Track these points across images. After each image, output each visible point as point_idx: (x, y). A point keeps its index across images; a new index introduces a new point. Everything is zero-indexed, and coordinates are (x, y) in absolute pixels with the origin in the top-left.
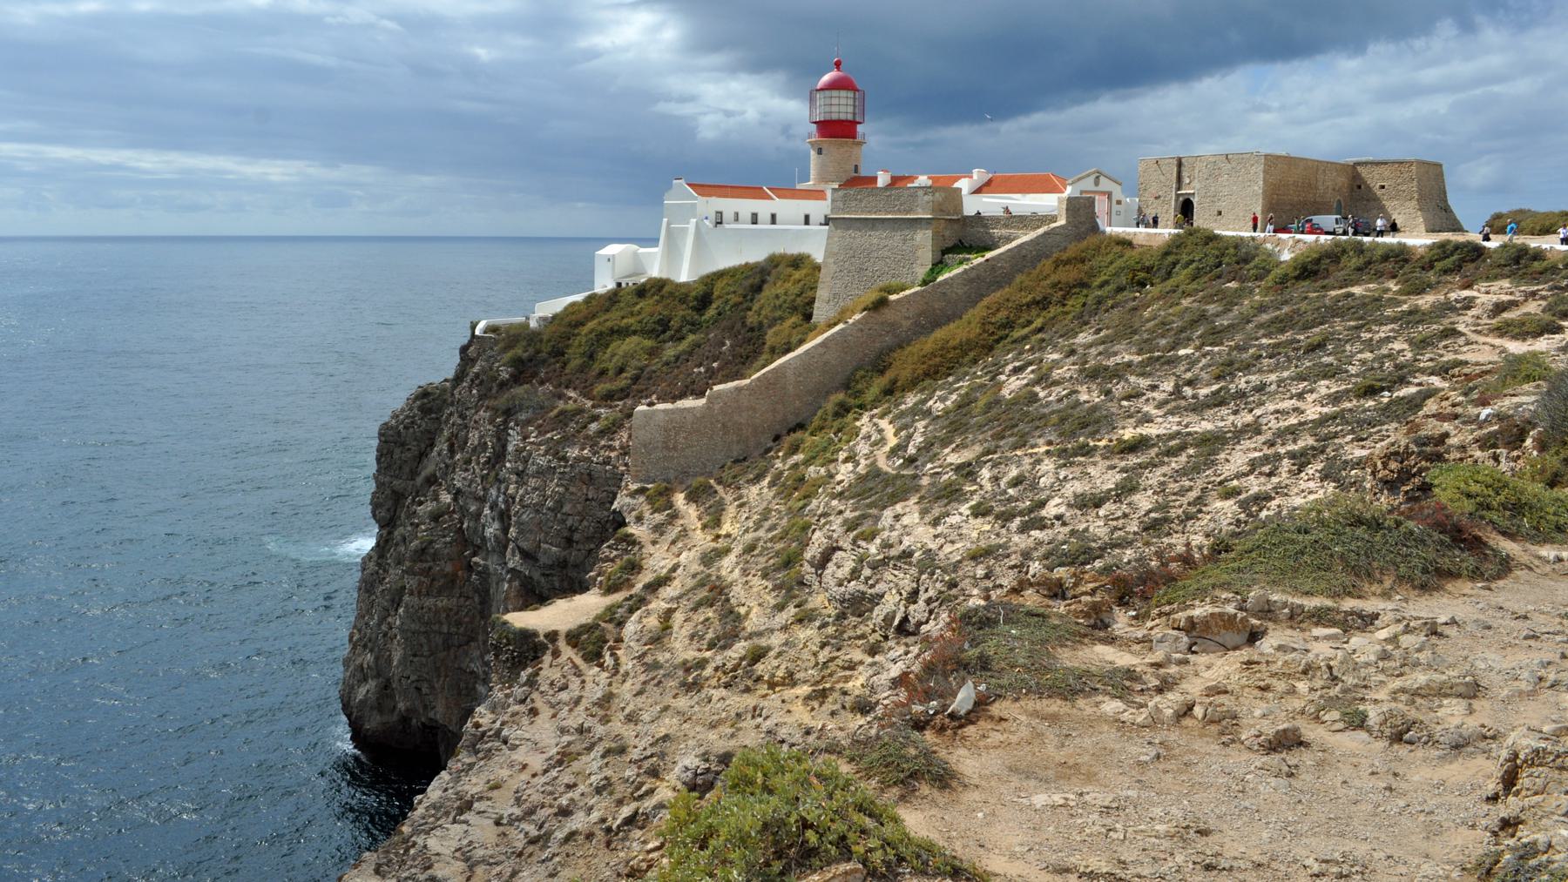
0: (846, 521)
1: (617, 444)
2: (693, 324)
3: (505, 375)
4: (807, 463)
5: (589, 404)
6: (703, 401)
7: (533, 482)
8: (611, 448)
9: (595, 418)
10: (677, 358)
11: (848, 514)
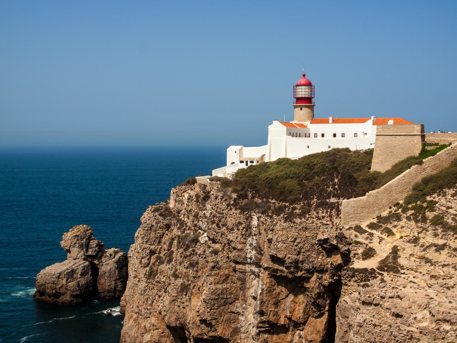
1: (314, 216)
3: (234, 196)
5: (287, 204)
6: (365, 197)
7: (281, 233)
8: (313, 218)
9: (295, 208)
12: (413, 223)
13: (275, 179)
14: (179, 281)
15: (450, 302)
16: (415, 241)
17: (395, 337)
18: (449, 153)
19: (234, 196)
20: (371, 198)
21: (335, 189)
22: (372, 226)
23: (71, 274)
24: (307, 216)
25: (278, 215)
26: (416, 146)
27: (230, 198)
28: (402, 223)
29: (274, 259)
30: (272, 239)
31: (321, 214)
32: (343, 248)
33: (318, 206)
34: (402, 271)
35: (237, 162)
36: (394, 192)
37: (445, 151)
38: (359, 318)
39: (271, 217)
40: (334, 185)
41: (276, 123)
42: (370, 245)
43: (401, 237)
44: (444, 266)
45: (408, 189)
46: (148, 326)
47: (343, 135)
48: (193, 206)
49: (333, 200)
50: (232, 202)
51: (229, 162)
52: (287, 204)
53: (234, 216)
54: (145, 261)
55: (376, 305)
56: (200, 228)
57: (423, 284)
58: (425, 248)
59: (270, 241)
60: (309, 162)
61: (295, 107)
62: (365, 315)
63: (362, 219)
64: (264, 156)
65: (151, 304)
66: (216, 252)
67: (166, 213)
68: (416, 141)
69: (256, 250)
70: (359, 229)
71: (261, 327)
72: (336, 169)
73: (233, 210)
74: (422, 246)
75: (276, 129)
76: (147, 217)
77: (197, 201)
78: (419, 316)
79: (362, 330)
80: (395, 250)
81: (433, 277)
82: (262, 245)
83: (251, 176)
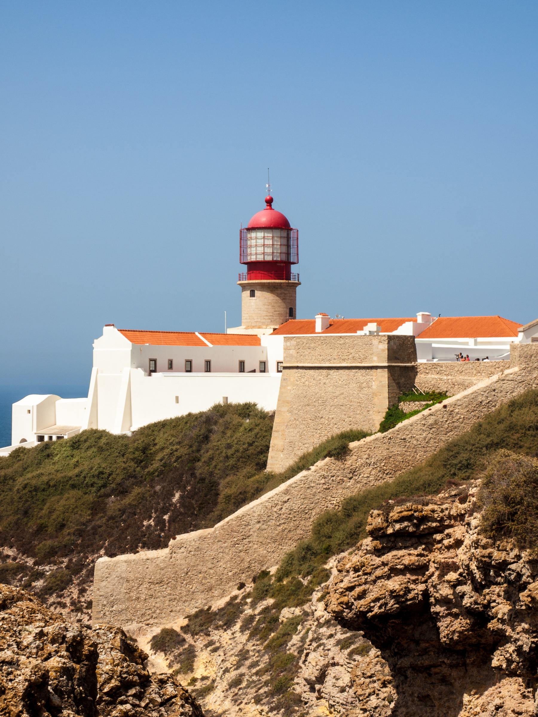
0: (338, 642)
1: (68, 601)
2: (135, 477)
4: (278, 606)
5: (30, 562)
8: (64, 606)
9: (40, 575)
10: (123, 511)
11: (340, 636)
13: (44, 490)
18: (436, 422)
20: (180, 555)
24: (51, 600)
26: (376, 400)
36: (254, 538)
37: (425, 418)
41: (111, 333)
45: (299, 532)
52: (30, 562)
61: (244, 287)
68: (374, 385)
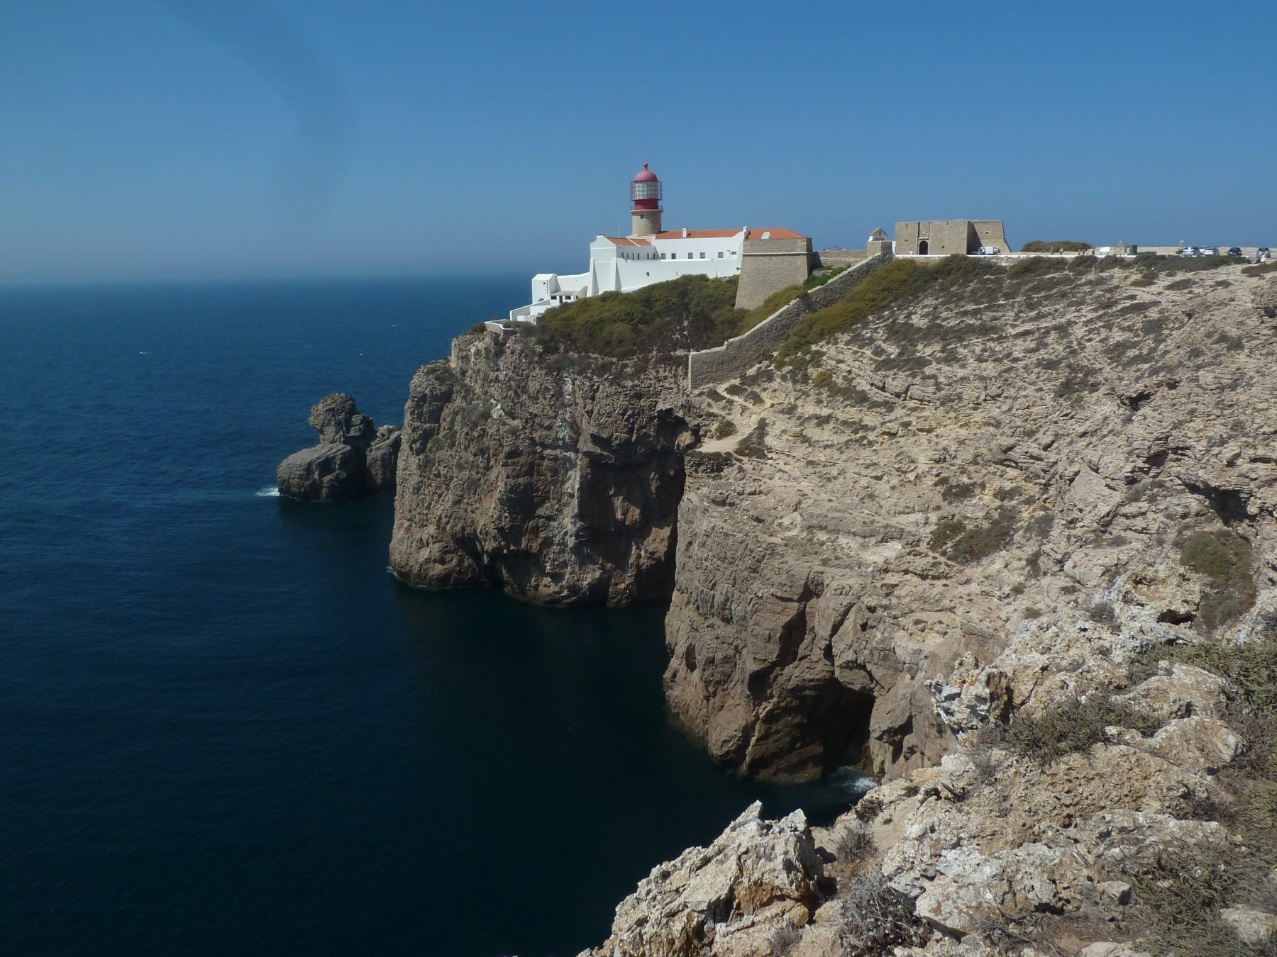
3: (539, 349)
5: (614, 360)
6: (724, 347)
7: (604, 402)
9: (626, 366)
12: (790, 384)
14: (465, 474)
15: (830, 500)
16: (791, 410)
17: (752, 551)
19: (539, 349)
21: (683, 336)
22: (733, 390)
23: (325, 465)
25: (600, 376)
27: (534, 352)
28: (775, 385)
29: (596, 439)
30: (592, 411)
31: (662, 374)
32: (693, 422)
33: (659, 361)
34: (770, 456)
35: (547, 298)
38: (704, 525)
39: (591, 379)
40: (683, 329)
42: (729, 418)
43: (772, 405)
44: (826, 447)
46: (425, 537)
47: (702, 256)
48: (482, 366)
49: (680, 352)
50: (536, 359)
51: (535, 298)
52: (614, 360)
53: (538, 379)
54: (417, 445)
55: (732, 505)
56: (492, 397)
57: (796, 473)
58: (803, 421)
59: (592, 411)
60: (648, 296)
61: (634, 214)
62: (716, 519)
63: (720, 380)
64: (585, 289)
65: (428, 508)
66: (514, 432)
67: (445, 376)
69: (572, 428)
70: (714, 395)
71: (582, 536)
72: (686, 306)
73: (537, 370)
74: (799, 418)
75: (602, 250)
76: (419, 381)
77: (487, 358)
78: (786, 521)
79: (709, 541)
80: (762, 425)
81: (810, 463)
82: (578, 421)
83: (566, 319)
